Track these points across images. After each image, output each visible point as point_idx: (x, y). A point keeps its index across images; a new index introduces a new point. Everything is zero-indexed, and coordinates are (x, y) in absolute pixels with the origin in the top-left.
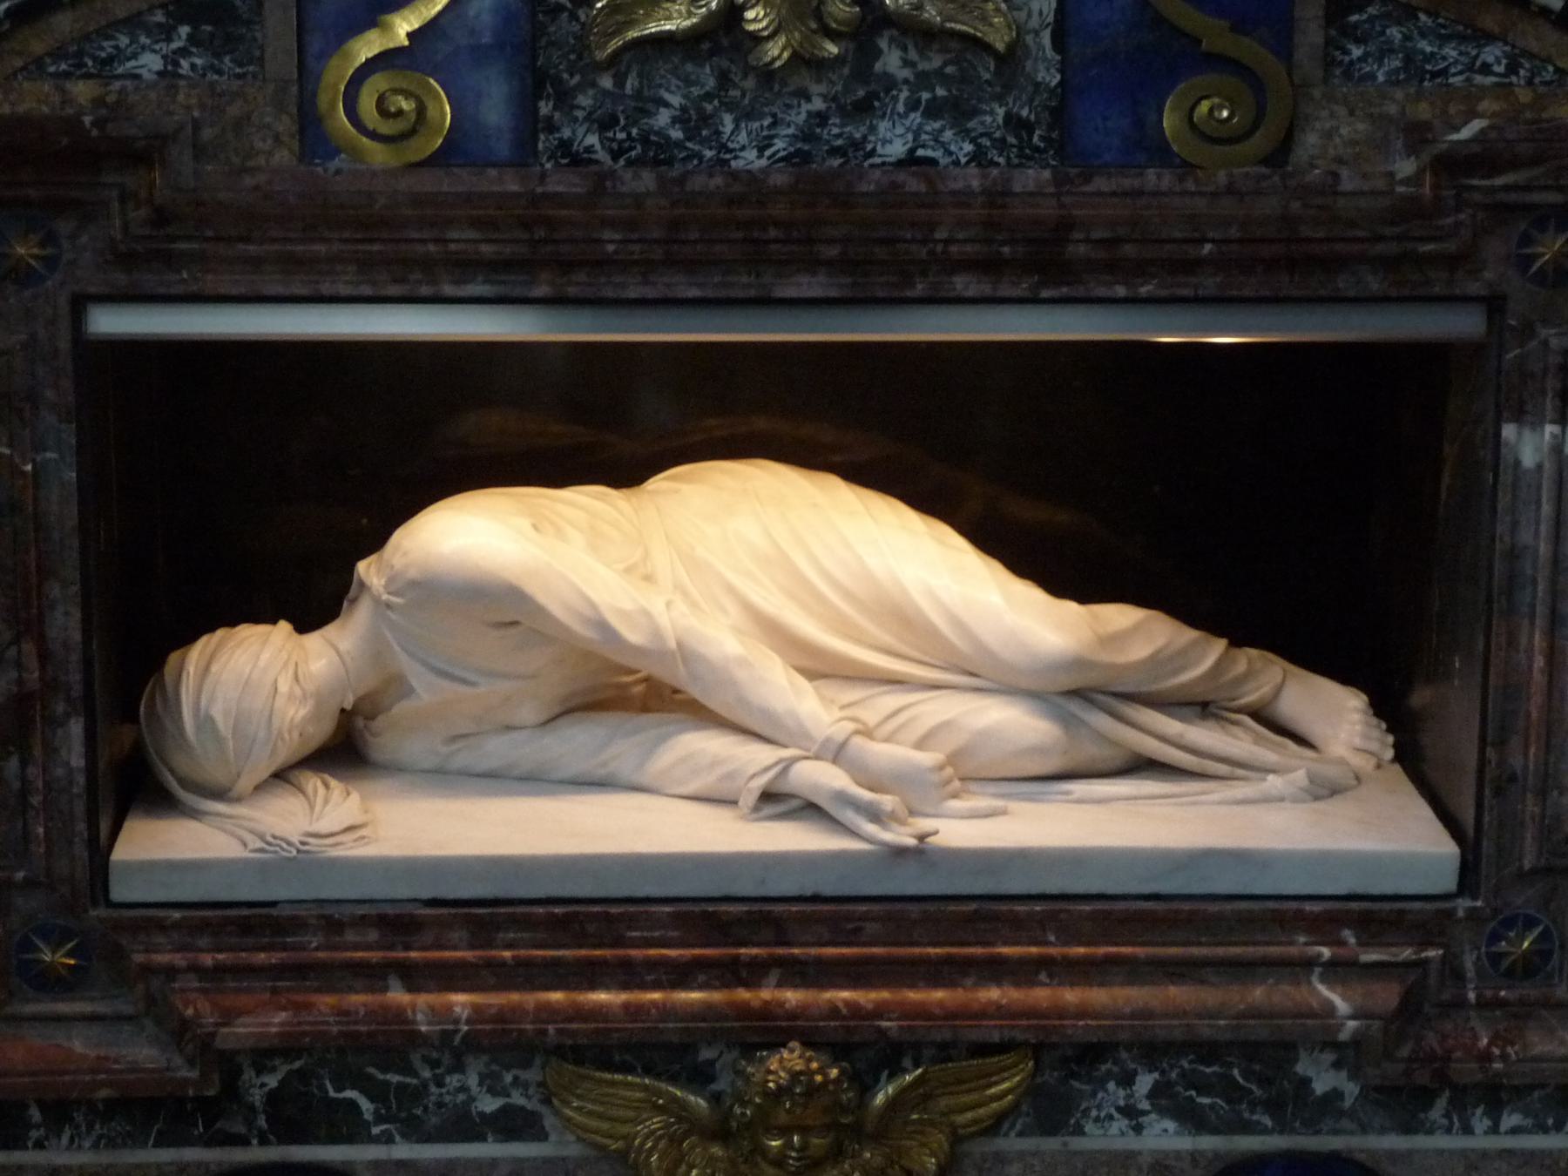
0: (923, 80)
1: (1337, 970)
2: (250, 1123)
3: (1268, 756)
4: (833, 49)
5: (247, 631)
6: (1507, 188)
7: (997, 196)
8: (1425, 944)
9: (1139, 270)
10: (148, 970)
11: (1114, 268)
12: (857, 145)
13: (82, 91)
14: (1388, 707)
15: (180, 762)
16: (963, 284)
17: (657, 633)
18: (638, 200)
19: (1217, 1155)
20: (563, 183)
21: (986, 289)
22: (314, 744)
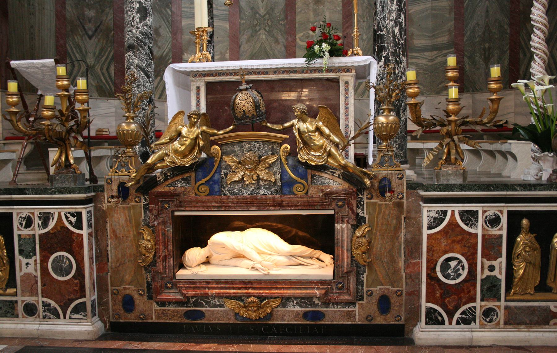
0: (265, 185)
1: (318, 289)
4: (254, 182)
7: (274, 198)
9: (292, 206)
10: (179, 287)
11: (289, 206)
13: (172, 188)
18: (233, 199)
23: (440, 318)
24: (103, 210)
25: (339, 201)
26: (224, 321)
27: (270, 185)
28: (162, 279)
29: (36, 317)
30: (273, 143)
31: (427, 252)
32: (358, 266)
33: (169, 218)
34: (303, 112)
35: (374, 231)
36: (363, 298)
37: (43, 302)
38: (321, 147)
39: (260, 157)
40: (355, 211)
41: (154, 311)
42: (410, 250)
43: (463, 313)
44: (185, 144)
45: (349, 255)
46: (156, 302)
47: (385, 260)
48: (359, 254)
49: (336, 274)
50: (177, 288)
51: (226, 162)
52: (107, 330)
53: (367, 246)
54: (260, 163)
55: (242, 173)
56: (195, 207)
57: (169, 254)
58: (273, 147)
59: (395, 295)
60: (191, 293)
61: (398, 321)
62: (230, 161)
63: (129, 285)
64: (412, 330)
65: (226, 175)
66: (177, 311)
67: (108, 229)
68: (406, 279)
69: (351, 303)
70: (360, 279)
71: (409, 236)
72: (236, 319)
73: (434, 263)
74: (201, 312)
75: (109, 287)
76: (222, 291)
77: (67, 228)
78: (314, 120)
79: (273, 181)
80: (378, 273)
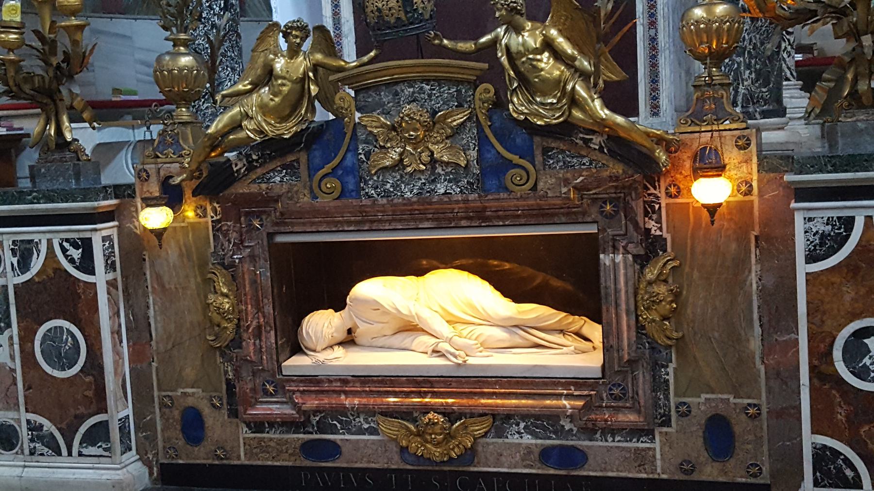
0: (447, 174)
1: (568, 397)
2: (313, 428)
3: (570, 343)
6: (594, 194)
7: (466, 201)
9: (506, 218)
11: (499, 218)
12: (433, 190)
13: (264, 186)
16: (464, 223)
17: (410, 312)
18: (383, 205)
19: (542, 445)
20: (365, 201)
21: (469, 224)
23: (849, 473)
24: (136, 234)
27: (456, 173)
28: (254, 374)
29: (17, 453)
30: (458, 82)
31: (808, 315)
33: (262, 247)
37: (28, 422)
40: (641, 225)
42: (773, 311)
44: (280, 92)
45: (633, 322)
46: (245, 422)
47: (716, 334)
48: (654, 321)
49: (606, 365)
50: (285, 393)
51: (365, 126)
52: (154, 481)
56: (313, 224)
57: (267, 323)
58: (459, 91)
59: (743, 417)
60: (311, 403)
61: (755, 476)
62: (374, 124)
63: (192, 387)
65: (368, 155)
68: (767, 378)
69: (643, 430)
70: (660, 377)
71: (770, 281)
74: (333, 443)
75: (156, 394)
76: (372, 401)
77: (66, 271)
80: (701, 363)
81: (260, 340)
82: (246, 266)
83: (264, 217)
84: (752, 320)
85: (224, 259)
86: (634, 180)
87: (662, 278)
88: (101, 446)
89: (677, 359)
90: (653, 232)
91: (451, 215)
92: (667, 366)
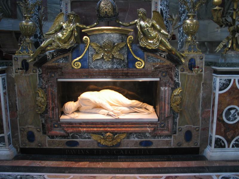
0: (117, 62)
1: (149, 127)
3: (145, 111)
5: (70, 102)
7: (123, 70)
8: (156, 125)
10: (62, 126)
13: (57, 64)
14: (155, 108)
15: (65, 111)
16: (121, 77)
17: (99, 103)
18: (96, 71)
19: (140, 141)
22: (75, 110)
23: (223, 144)
25: (163, 72)
26: (91, 147)
28: (51, 121)
31: (218, 105)
32: (174, 113)
34: (144, 14)
35: (184, 92)
36: (176, 132)
38: (154, 38)
39: (114, 44)
41: (47, 141)
43: (237, 141)
45: (169, 107)
48: (175, 106)
50: (61, 127)
53: (180, 101)
54: (114, 47)
55: (103, 54)
57: (55, 106)
58: (122, 37)
59: (195, 130)
60: (70, 130)
61: (196, 145)
63: (31, 125)
64: (203, 151)
65: (92, 55)
66: (61, 141)
67: (16, 90)
68: (202, 121)
69: (169, 136)
71: (205, 95)
72: (98, 146)
73: (222, 111)
75: (19, 127)
78: (150, 19)
79: (123, 59)
81: (54, 111)
82: (50, 89)
83: (56, 73)
84: (199, 105)
85: (42, 86)
86: (173, 66)
87: (178, 94)
88: (2, 144)
89: (180, 116)
90: (176, 81)
91: (117, 75)
92: (177, 118)
